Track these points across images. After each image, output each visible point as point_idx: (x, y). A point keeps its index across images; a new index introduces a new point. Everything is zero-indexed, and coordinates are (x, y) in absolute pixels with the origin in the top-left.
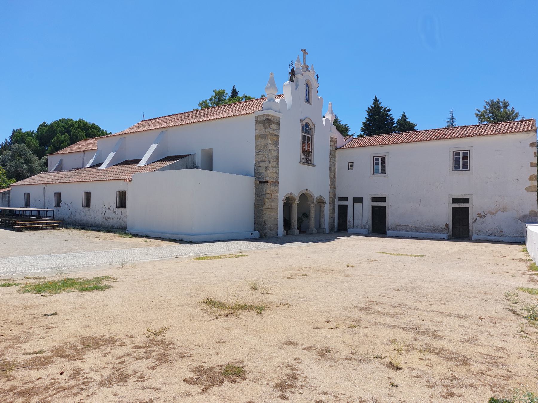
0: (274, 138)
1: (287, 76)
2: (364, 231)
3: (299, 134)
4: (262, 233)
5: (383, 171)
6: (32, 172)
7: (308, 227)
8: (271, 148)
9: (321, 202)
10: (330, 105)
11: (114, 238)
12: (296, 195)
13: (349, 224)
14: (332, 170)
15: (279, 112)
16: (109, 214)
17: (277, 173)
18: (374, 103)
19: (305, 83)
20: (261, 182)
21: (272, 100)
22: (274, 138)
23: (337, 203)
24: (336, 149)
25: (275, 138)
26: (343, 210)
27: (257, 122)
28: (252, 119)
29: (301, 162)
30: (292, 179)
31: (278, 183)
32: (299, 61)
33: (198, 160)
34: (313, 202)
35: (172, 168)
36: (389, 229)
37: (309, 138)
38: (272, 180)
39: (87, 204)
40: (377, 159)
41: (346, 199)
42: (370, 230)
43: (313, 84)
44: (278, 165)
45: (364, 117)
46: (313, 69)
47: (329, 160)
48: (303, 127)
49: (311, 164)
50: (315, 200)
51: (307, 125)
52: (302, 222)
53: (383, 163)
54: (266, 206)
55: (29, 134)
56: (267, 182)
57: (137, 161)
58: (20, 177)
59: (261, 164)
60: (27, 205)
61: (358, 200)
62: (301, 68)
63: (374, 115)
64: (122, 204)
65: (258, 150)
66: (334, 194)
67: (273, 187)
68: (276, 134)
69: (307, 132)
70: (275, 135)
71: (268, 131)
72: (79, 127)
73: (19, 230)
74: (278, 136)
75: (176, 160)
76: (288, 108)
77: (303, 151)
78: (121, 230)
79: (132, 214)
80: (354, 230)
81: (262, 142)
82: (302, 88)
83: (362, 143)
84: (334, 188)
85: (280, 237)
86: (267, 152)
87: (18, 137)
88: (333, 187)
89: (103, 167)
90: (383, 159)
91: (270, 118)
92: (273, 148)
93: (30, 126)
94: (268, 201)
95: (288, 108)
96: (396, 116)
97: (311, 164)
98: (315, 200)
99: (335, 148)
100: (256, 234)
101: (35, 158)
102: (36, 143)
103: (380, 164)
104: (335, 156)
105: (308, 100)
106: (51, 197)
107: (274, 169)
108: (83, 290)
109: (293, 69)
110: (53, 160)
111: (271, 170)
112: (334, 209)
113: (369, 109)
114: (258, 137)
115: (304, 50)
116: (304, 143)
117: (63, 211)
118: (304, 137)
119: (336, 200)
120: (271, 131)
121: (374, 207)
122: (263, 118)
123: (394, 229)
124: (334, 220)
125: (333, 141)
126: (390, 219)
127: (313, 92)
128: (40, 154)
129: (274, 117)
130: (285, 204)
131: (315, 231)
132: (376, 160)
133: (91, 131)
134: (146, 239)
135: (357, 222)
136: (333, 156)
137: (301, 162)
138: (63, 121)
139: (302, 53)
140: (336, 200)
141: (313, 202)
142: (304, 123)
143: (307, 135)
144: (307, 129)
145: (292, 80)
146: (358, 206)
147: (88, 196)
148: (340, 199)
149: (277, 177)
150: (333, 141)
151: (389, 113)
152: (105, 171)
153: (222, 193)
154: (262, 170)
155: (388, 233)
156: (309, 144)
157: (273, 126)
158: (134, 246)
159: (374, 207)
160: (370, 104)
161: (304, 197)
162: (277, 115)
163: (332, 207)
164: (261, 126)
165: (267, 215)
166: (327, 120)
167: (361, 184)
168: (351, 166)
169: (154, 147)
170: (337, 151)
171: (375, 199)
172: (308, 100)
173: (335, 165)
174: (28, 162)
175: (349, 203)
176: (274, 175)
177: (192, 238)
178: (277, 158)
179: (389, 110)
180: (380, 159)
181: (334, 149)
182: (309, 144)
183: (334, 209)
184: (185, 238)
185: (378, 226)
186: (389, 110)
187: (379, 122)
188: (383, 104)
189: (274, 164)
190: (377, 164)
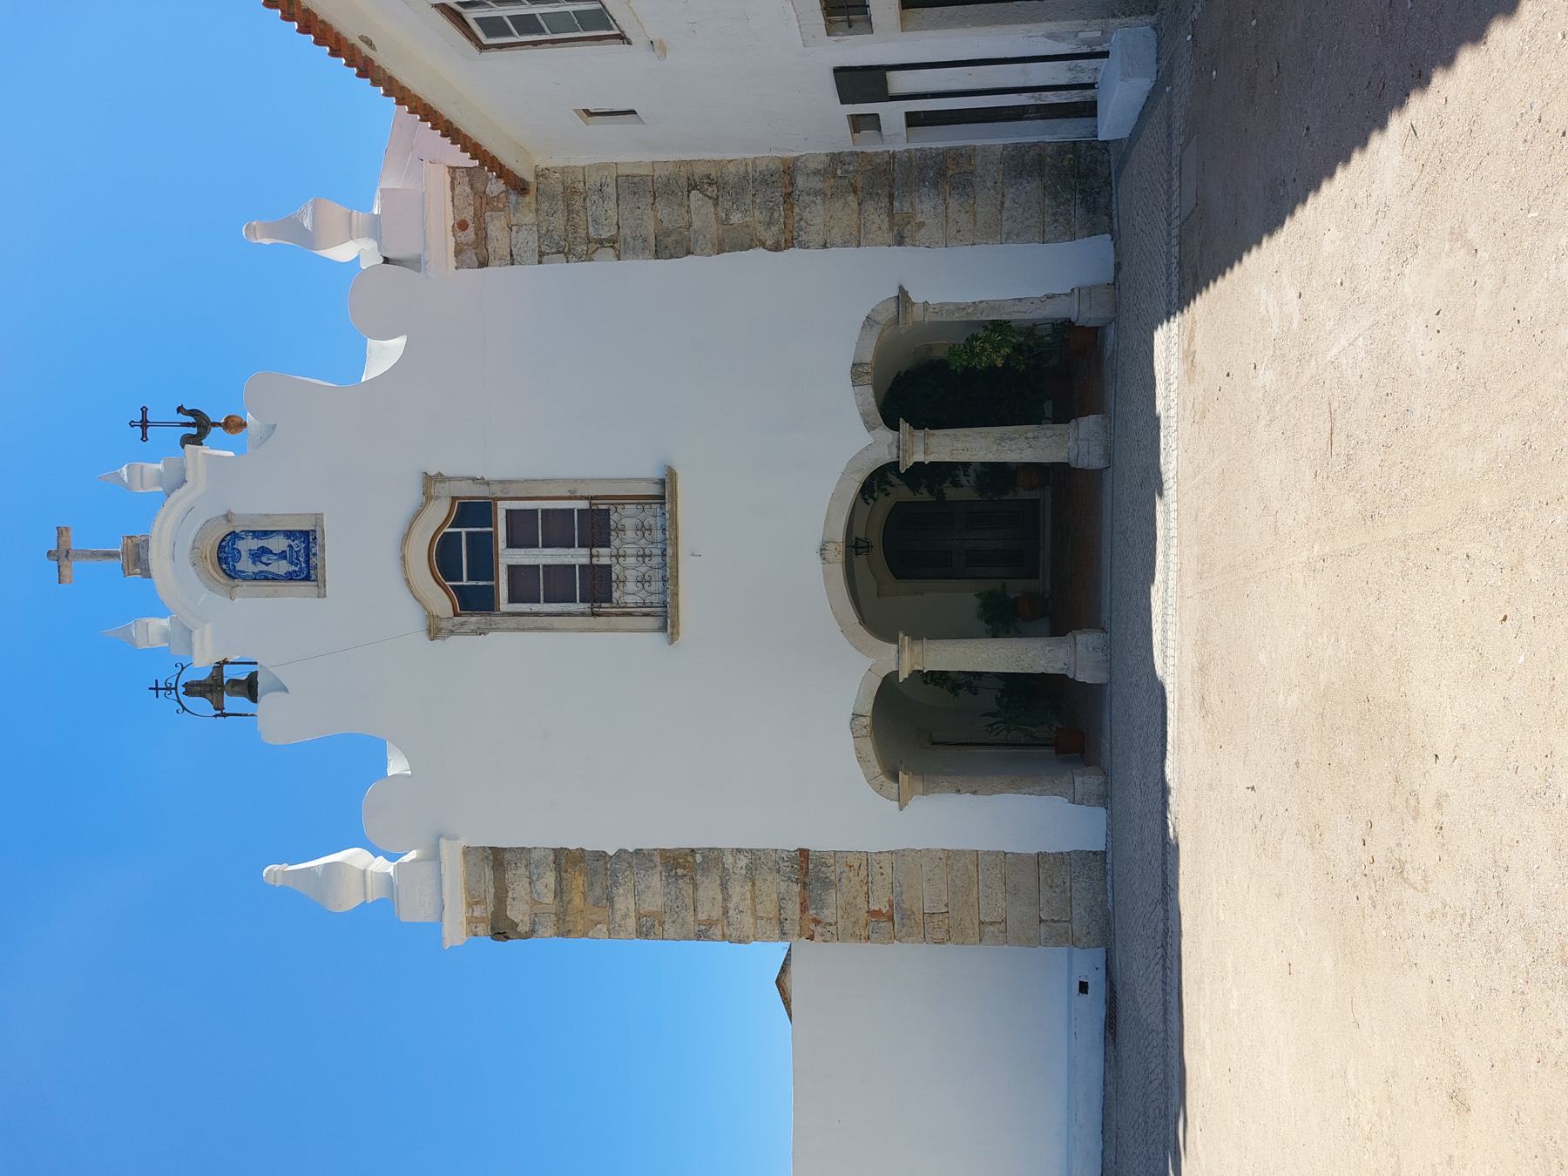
0: (578, 901)
15: (434, 856)
17: (756, 860)
22: (578, 901)
25: (578, 882)
29: (663, 615)
31: (804, 853)
47: (604, 268)
61: (860, 83)
68: (550, 878)
74: (565, 860)
77: (595, 590)
85: (1111, 833)
107: (738, 891)
118: (524, 584)
119: (869, 144)
124: (1020, 163)
137: (663, 615)
139: (76, 567)
142: (442, 603)
143: (507, 557)
146: (899, 82)
162: (452, 856)
163: (925, 207)
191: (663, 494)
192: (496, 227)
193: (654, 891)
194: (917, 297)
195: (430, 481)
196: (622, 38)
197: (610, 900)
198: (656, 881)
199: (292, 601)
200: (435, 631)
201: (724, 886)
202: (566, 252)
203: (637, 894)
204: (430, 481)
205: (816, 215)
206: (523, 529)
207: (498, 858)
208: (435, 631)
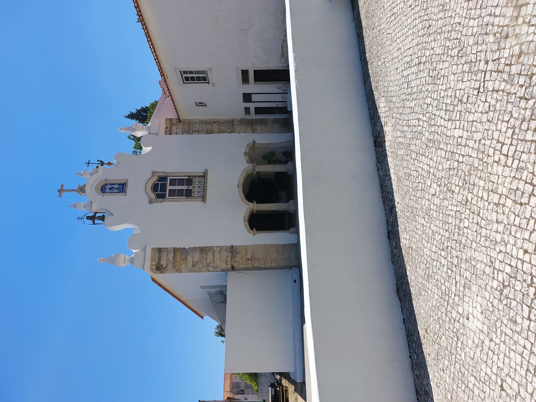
0: (178, 259)
8: (191, 264)
10: (123, 131)
12: (245, 208)
13: (280, 105)
15: (145, 250)
17: (221, 248)
22: (178, 259)
23: (253, 116)
25: (178, 255)
31: (232, 246)
34: (254, 170)
37: (173, 182)
44: (211, 249)
47: (196, 135)
49: (204, 176)
61: (247, 97)
66: (242, 122)
67: (238, 258)
68: (172, 254)
74: (175, 250)
77: (188, 194)
84: (233, 121)
91: (154, 267)
97: (204, 176)
104: (190, 123)
115: (59, 191)
118: (172, 193)
119: (248, 117)
121: (256, 80)
124: (275, 121)
135: (278, 98)
137: (204, 198)
139: (64, 194)
140: (248, 117)
142: (153, 196)
143: (169, 187)
146: (254, 98)
163: (258, 127)
191: (204, 176)
192: (174, 128)
193: (197, 256)
194: (257, 142)
195: (154, 173)
196: (209, 83)
197: (186, 259)
198: (197, 254)
199: (119, 197)
200: (151, 202)
201: (213, 254)
202: (188, 133)
203: (193, 257)
204: (154, 173)
205: (238, 128)
206: (173, 182)
207: (160, 250)
208: (151, 202)
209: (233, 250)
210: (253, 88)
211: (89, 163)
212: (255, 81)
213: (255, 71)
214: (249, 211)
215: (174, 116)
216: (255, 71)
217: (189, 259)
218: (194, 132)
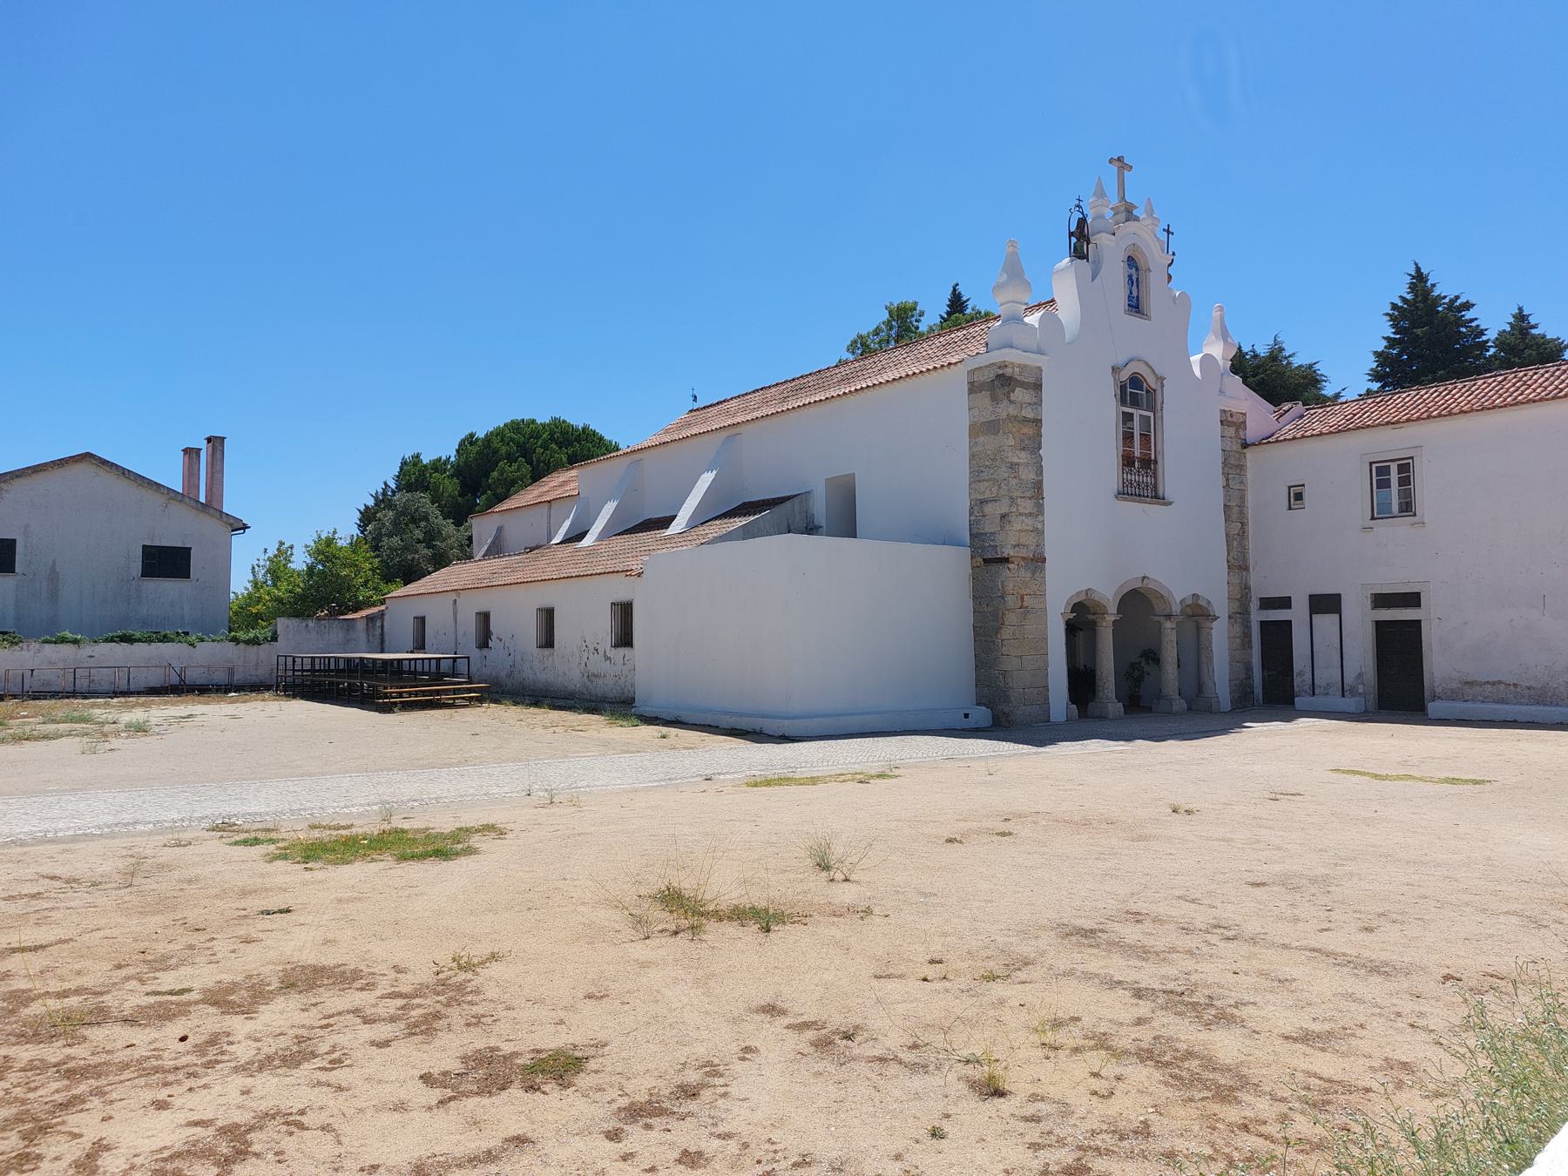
0: (1025, 430)
1: (1063, 243)
2: (1349, 703)
3: (1108, 410)
4: (998, 711)
5: (1407, 507)
6: (440, 561)
7: (1159, 695)
8: (1015, 460)
9: (1197, 614)
10: (1216, 314)
11: (596, 726)
12: (1108, 594)
13: (1300, 681)
14: (1235, 513)
15: (1040, 352)
16: (597, 664)
17: (1040, 533)
18: (1413, 288)
19: (1123, 256)
20: (988, 561)
21: (1017, 319)
22: (1025, 430)
23: (1257, 616)
24: (1245, 445)
25: (1029, 430)
26: (1277, 638)
27: (973, 388)
28: (958, 380)
30: (1088, 545)
31: (1044, 560)
32: (1100, 193)
33: (820, 509)
34: (1169, 616)
35: (747, 533)
36: (1434, 698)
37: (1145, 421)
38: (1023, 553)
39: (548, 641)
40: (1383, 471)
41: (1285, 603)
42: (1372, 699)
43: (1154, 257)
45: (1378, 333)
46: (1150, 212)
47: (1221, 481)
48: (1123, 388)
49: (1156, 497)
50: (1176, 609)
51: (1136, 381)
52: (1127, 676)
53: (1405, 481)
54: (1006, 633)
55: (438, 466)
56: (1006, 560)
57: (665, 522)
58: (410, 574)
59: (988, 509)
60: (420, 646)
61: (1326, 604)
62: (1109, 214)
63: (1414, 325)
64: (624, 638)
65: (979, 468)
66: (1246, 588)
67: (1025, 574)
68: (1031, 416)
69: (1135, 402)
70: (1026, 420)
71: (1005, 409)
72: (552, 439)
73: (387, 709)
74: (1038, 422)
75: (758, 511)
76: (1068, 336)
77: (1128, 461)
78: (619, 705)
79: (650, 664)
80: (1319, 702)
81: (989, 443)
82: (1115, 273)
83: (1333, 421)
84: (1246, 568)
85: (1056, 724)
86: (1003, 472)
87: (414, 476)
88: (1239, 564)
89: (588, 541)
90: (1405, 468)
91: (1008, 371)
92: (1023, 457)
93: (441, 446)
94: (1011, 618)
95: (1068, 336)
96: (1492, 321)
97: (1156, 497)
98: (1176, 609)
99: (1239, 445)
100: (982, 715)
101: (448, 527)
102: (451, 487)
103: (1394, 486)
104: (1241, 468)
105: (1135, 306)
106: (469, 626)
107: (1029, 521)
108: (403, 858)
109: (1082, 222)
110: (482, 527)
111: (1017, 524)
112: (1246, 635)
113: (1394, 307)
114: (976, 430)
115: (1120, 159)
116: (1128, 437)
117: (495, 661)
118: (1128, 417)
119: (1254, 605)
120: (1012, 410)
121: (1379, 625)
122: (989, 376)
123: (1453, 696)
124: (1248, 668)
125: (1231, 421)
126: (1440, 663)
127: (1154, 282)
128: (460, 515)
129: (1023, 367)
130: (1071, 628)
131: (1179, 704)
132: (1380, 475)
133: (576, 446)
134: (665, 730)
135: (1327, 673)
136: (1233, 467)
138: (515, 426)
139: (1114, 169)
140: (1254, 605)
141: (1169, 616)
143: (1137, 413)
144: (1136, 393)
145: (1079, 254)
146: (1325, 622)
147: (548, 615)
148: (1268, 603)
149: (1040, 545)
150: (1231, 421)
151: (1468, 315)
152: (591, 551)
153: (885, 597)
154: (989, 527)
155: (1433, 708)
156: (1145, 438)
157: (1019, 394)
158: (629, 749)
159: (1379, 625)
160: (1400, 289)
161: (1137, 601)
162: (1032, 360)
163: (1238, 629)
164: (984, 398)
165: (1013, 658)
166: (1207, 360)
167: (1336, 552)
168: (1299, 497)
169: (707, 478)
170: (1250, 454)
171: (1381, 601)
172: (1135, 306)
173: (1242, 498)
174: (431, 537)
175: (1298, 614)
176: (1030, 540)
177: (787, 727)
178: (1038, 486)
179: (1468, 306)
180: (1394, 468)
181: (1236, 447)
182: (1145, 438)
183: (1246, 635)
184: (770, 726)
185: (1399, 683)
186: (1468, 306)
187: (1431, 345)
188: (1445, 287)
189: (1027, 506)
190: (1384, 484)
191: (1157, 497)
192: (1232, 430)
193: (1027, 475)
195: (1161, 379)
196: (1373, 518)
197: (1023, 449)
198: (1032, 476)
201: (1031, 514)
203: (1027, 465)
204: (1161, 379)
205: (1236, 581)
207: (1038, 386)
208: (1115, 370)
209: (1038, 561)
210: (1359, 621)
211: (1168, 232)
212: (1377, 622)
213: (1417, 624)
214: (1098, 604)
215: (1252, 434)
216: (1417, 624)
217: (1023, 454)
218: (1226, 475)
